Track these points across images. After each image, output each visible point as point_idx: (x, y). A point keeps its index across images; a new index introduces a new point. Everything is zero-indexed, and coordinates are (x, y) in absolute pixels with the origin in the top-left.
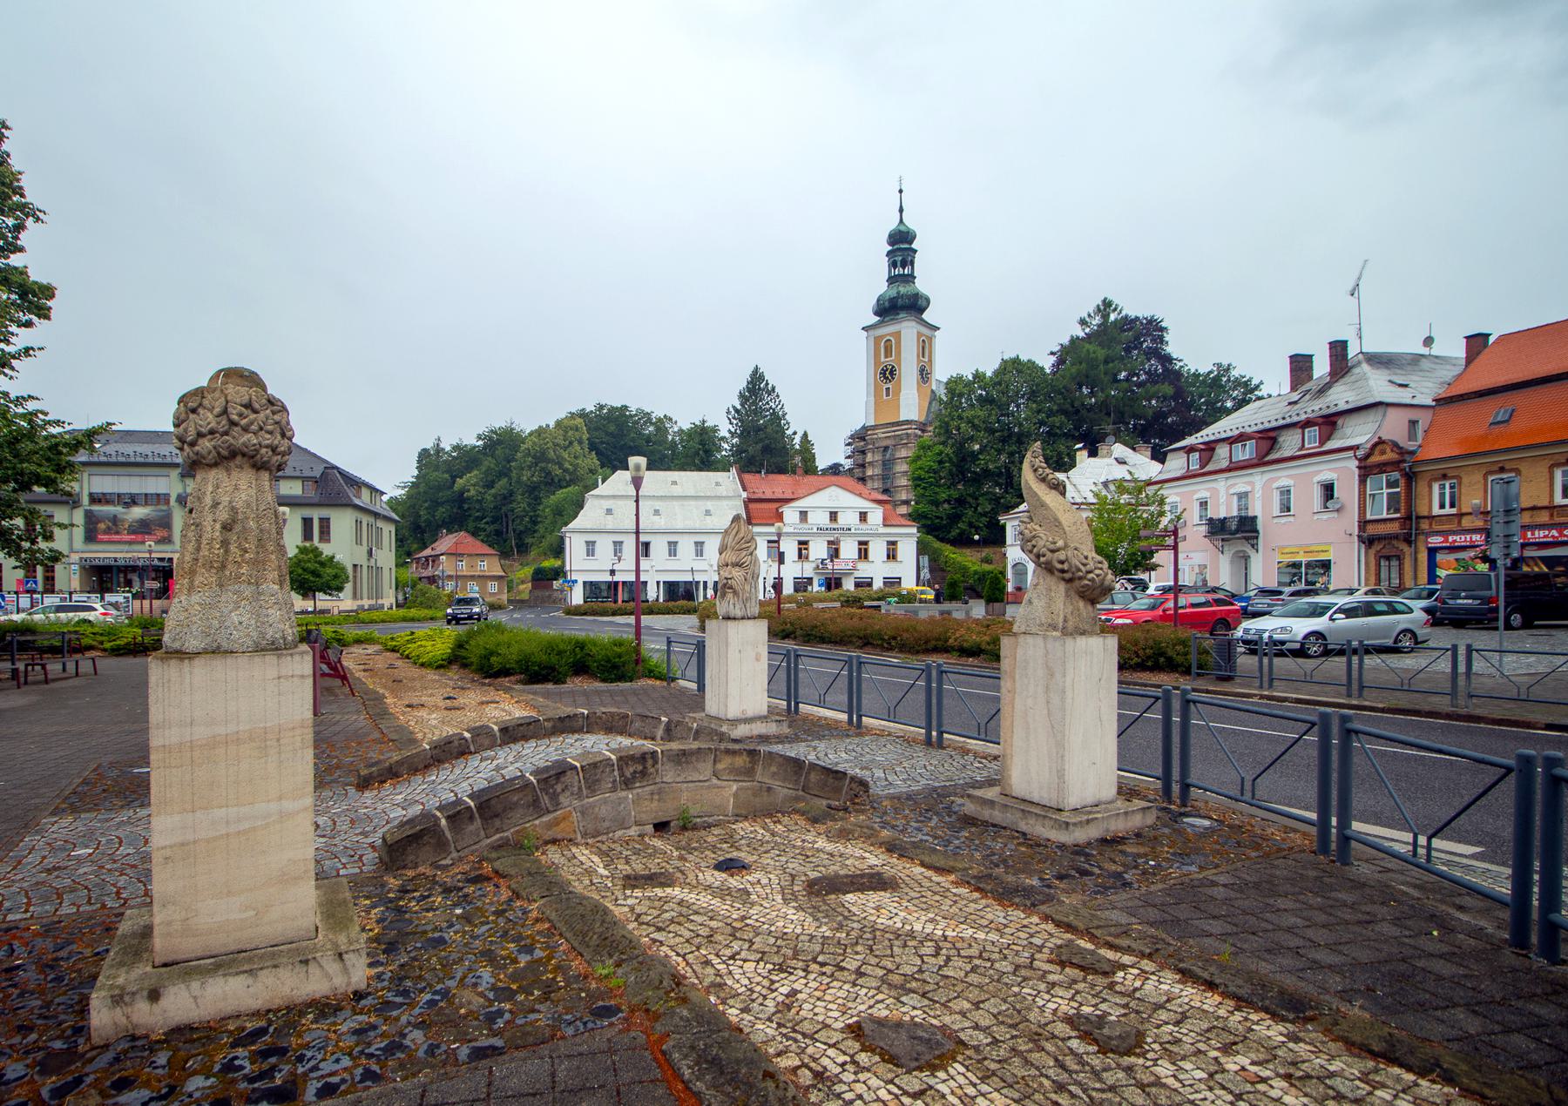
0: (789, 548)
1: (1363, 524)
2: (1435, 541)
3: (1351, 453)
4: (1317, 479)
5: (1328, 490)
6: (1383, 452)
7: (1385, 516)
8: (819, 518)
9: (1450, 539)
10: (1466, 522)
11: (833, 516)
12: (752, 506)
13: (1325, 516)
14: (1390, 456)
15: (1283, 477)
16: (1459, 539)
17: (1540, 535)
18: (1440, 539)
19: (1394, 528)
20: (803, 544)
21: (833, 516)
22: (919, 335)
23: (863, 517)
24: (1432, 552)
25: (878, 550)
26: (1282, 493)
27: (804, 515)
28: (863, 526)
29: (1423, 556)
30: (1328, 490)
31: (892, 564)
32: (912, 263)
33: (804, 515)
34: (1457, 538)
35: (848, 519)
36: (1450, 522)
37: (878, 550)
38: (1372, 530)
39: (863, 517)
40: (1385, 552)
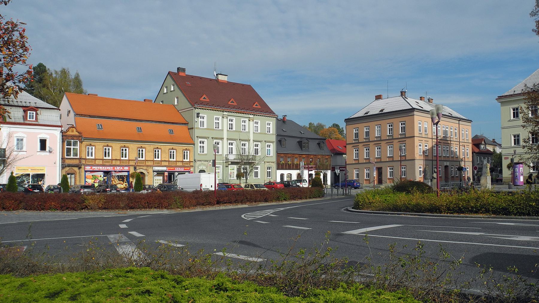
1: (63, 159)
2: (88, 168)
3: (60, 129)
4: (15, 135)
5: (43, 143)
6: (73, 131)
7: (72, 157)
9: (93, 168)
10: (97, 162)
13: (43, 153)
14: (75, 133)
15: (20, 132)
16: (96, 168)
17: (118, 169)
18: (89, 168)
19: (76, 162)
24: (86, 171)
26: (18, 140)
29: (83, 173)
30: (43, 143)
34: (95, 168)
36: (92, 162)
38: (67, 162)
40: (70, 172)
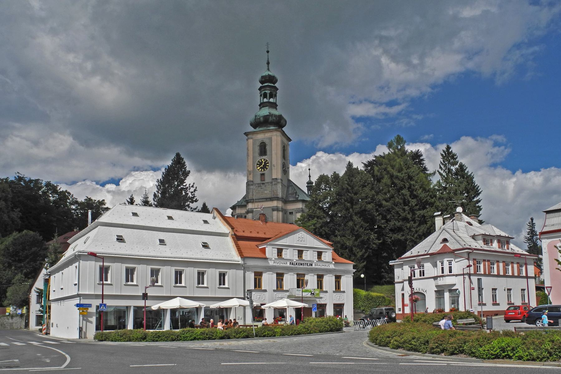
0: (269, 280)
8: (290, 254)
11: (300, 253)
12: (241, 243)
20: (280, 277)
21: (300, 253)
22: (282, 142)
23: (320, 254)
25: (329, 281)
27: (280, 252)
28: (321, 264)
31: (338, 295)
32: (276, 96)
33: (280, 252)
35: (309, 256)
37: (329, 281)
39: (320, 254)
